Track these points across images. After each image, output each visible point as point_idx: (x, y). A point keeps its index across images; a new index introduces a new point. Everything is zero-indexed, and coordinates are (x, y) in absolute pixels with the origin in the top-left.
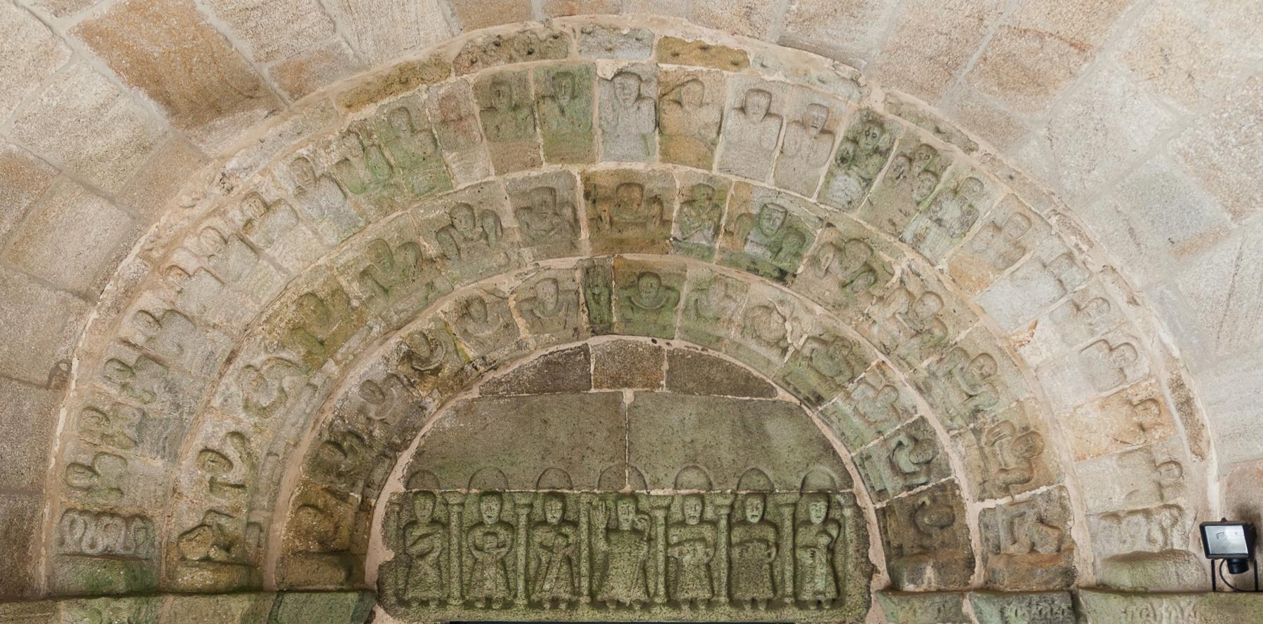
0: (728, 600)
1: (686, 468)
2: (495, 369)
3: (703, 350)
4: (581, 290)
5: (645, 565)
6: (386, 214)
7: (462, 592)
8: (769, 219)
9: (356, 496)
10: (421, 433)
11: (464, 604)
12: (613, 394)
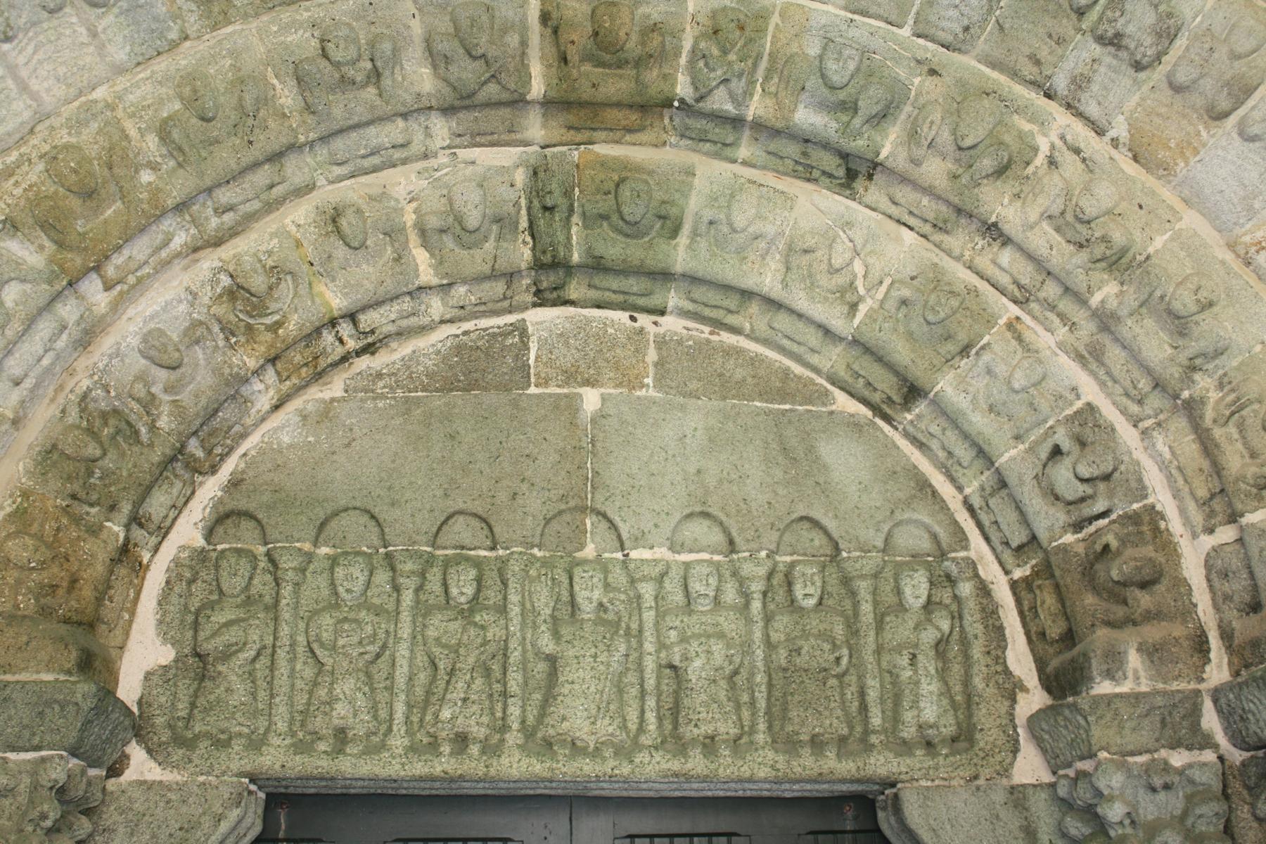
0: (769, 740)
1: (690, 516)
2: (369, 349)
3: (711, 333)
4: (523, 202)
5: (620, 681)
6: (215, 27)
7: (291, 723)
8: (838, 60)
9: (116, 528)
10: (241, 451)
11: (293, 745)
12: (566, 396)
